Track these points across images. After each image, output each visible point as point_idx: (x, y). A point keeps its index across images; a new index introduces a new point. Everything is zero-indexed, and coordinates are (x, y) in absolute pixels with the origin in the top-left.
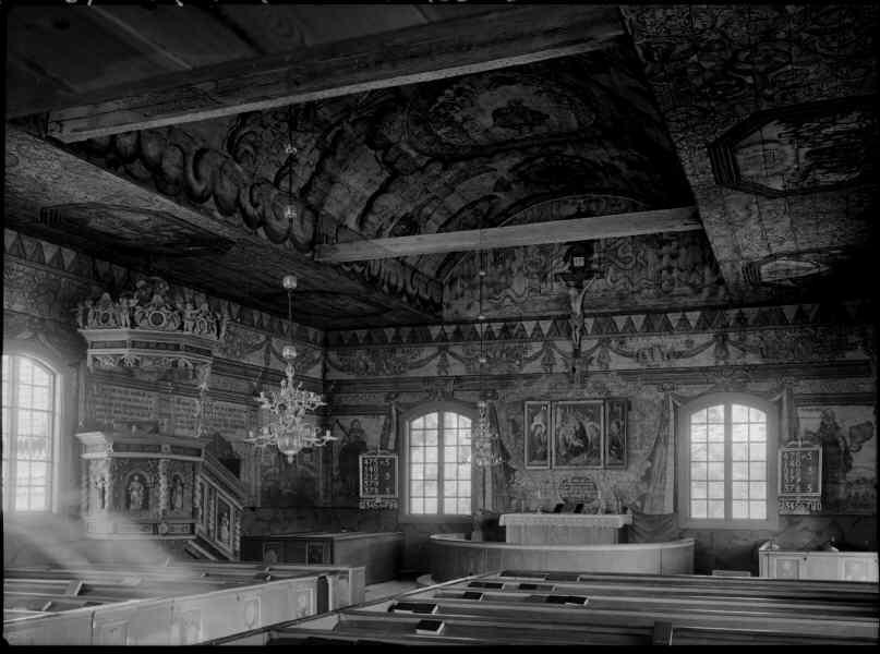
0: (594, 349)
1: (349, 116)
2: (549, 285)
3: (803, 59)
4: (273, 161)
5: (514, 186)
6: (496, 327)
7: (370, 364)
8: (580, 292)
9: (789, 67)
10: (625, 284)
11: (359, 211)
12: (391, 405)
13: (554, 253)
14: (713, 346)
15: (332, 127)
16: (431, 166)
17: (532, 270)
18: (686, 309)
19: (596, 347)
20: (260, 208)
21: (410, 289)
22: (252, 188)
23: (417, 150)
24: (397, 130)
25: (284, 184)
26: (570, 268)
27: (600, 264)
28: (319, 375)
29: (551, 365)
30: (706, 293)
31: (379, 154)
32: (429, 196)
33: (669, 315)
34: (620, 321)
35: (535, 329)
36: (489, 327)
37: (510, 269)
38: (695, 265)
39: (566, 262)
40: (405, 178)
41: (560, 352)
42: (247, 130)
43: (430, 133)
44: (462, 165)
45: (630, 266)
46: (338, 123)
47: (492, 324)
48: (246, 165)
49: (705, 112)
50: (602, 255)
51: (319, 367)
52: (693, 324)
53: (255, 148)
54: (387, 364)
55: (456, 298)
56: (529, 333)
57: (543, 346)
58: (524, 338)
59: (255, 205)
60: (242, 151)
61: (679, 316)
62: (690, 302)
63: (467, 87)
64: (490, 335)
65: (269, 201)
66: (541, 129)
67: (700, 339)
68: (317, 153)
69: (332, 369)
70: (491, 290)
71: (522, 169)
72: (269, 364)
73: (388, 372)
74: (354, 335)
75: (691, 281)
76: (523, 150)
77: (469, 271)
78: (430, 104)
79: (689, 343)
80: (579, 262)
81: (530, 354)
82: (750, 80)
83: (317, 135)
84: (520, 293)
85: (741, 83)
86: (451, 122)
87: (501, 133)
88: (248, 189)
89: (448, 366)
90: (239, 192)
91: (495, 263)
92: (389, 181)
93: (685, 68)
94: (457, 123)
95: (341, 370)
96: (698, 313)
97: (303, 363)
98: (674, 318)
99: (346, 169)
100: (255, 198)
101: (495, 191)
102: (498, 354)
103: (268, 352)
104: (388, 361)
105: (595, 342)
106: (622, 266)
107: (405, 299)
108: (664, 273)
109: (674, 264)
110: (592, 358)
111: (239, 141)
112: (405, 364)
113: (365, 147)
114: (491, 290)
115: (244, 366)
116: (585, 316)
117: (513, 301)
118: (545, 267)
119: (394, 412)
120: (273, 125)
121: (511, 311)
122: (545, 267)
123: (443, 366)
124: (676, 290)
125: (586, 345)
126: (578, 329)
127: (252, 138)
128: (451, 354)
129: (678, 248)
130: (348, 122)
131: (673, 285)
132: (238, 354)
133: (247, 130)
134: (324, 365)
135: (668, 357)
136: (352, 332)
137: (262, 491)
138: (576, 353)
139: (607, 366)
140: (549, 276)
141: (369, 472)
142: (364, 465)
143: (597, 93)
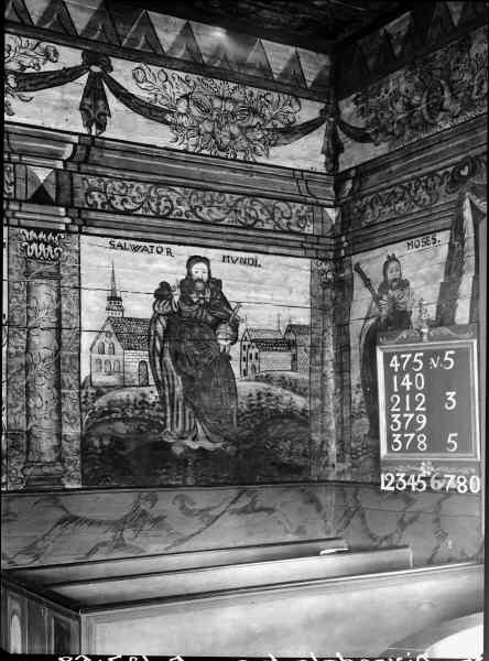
12: (460, 204)
28: (319, 163)
51: (317, 140)
72: (102, 127)
74: (388, 36)
95: (361, 137)
97: (244, 130)
119: (468, 214)
137: (85, 449)
141: (402, 391)
142: (389, 372)
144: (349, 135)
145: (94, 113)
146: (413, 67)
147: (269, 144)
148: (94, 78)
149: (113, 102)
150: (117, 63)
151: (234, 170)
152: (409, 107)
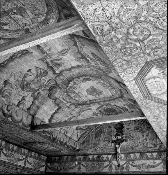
0: (124, 164)
1: (41, 88)
2: (111, 144)
3: (155, 33)
4: (17, 99)
5: (99, 115)
6: (95, 157)
7: (59, 167)
8: (120, 146)
9: (151, 37)
10: (133, 144)
11: (49, 117)
13: (112, 135)
14: (162, 165)
15: (36, 91)
16: (71, 106)
17: (106, 139)
18: (152, 152)
19: (126, 163)
20: (10, 112)
21: (68, 143)
22: (8, 106)
23: (65, 101)
24: (58, 94)
25: (21, 106)
26: (117, 139)
27: (125, 138)
29: (111, 169)
30: (158, 146)
31: (53, 101)
32: (72, 115)
33: (147, 154)
34: (132, 155)
35: (106, 158)
36: (93, 157)
37: (99, 139)
38: (154, 138)
39: (116, 137)
40: (63, 109)
41: (114, 165)
42: (7, 88)
43: (69, 96)
44: (81, 106)
45: (134, 138)
46: (38, 90)
47: (94, 156)
48: (7, 99)
49: (128, 62)
50: (126, 135)
51: (44, 168)
52: (155, 157)
53: (10, 94)
54: (63, 167)
55: (84, 148)
56: (105, 159)
57: (109, 163)
58: (103, 161)
59: (9, 111)
60: (5, 94)
61: (150, 154)
62: (153, 149)
63: (77, 82)
64: (93, 158)
65: (15, 110)
66: (102, 96)
67: (158, 162)
68: (32, 99)
69: (48, 169)
70: (94, 146)
71: (100, 109)
73: (64, 170)
74: (55, 158)
75: (153, 143)
76: (98, 103)
77: (88, 140)
78: (67, 86)
79: (154, 163)
80: (119, 137)
81: (105, 165)
82: (138, 44)
83: (32, 93)
84: (102, 146)
85: (136, 47)
86: (74, 93)
87: (91, 97)
88: (6, 106)
89: (81, 169)
90: (2, 106)
91: (96, 137)
92: (58, 110)
93: (112, 39)
94: (76, 93)
95: (50, 168)
96: (156, 153)
97: (38, 166)
98: (149, 155)
99: (43, 104)
100: (9, 108)
101: (93, 115)
102: (95, 165)
103: (25, 161)
104: (64, 167)
105: (125, 162)
106: (132, 138)
107: (66, 146)
108: (145, 140)
109: (147, 138)
110: (124, 167)
111: (4, 91)
112: (68, 167)
113: (48, 98)
114: (94, 146)
115: (16, 166)
116: (122, 153)
117: (100, 149)
118: (109, 139)
120: (16, 88)
121: (99, 151)
122: (109, 139)
123: (79, 168)
124: (149, 146)
125: (122, 163)
126: (119, 157)
127: (9, 91)
128: (82, 165)
129: (148, 133)
130: (41, 90)
131: (148, 144)
132: (14, 161)
133: (5, 88)
134: (46, 167)
135: (148, 167)
136: (55, 157)
138: (119, 165)
139: (129, 170)
140: (111, 141)
143: (113, 82)
144: (48, 168)
145: (25, 164)
146: (59, 163)
147: (40, 168)
148: (26, 160)
149: (27, 163)
150: (28, 158)
151: (36, 171)
152: (58, 168)
